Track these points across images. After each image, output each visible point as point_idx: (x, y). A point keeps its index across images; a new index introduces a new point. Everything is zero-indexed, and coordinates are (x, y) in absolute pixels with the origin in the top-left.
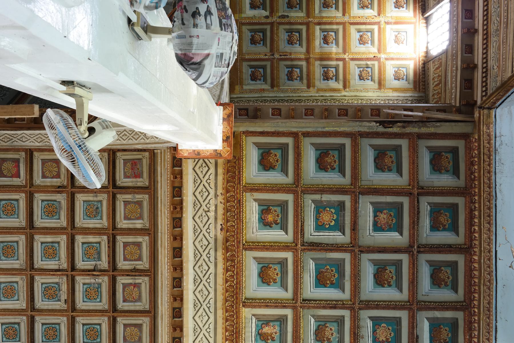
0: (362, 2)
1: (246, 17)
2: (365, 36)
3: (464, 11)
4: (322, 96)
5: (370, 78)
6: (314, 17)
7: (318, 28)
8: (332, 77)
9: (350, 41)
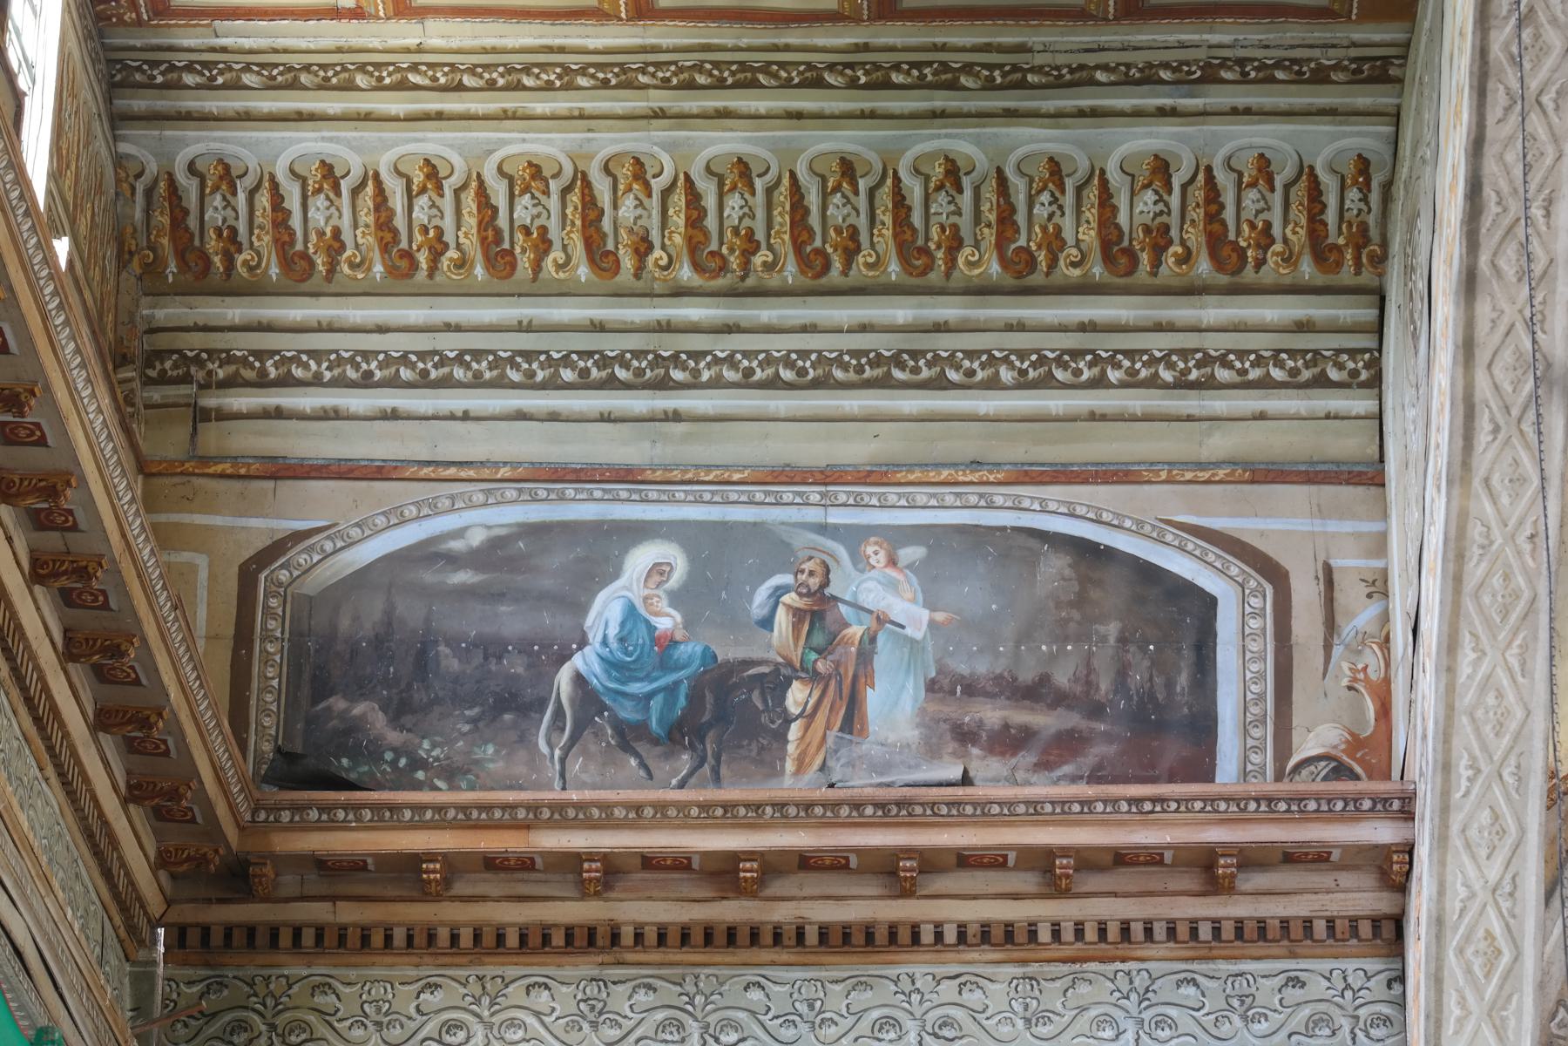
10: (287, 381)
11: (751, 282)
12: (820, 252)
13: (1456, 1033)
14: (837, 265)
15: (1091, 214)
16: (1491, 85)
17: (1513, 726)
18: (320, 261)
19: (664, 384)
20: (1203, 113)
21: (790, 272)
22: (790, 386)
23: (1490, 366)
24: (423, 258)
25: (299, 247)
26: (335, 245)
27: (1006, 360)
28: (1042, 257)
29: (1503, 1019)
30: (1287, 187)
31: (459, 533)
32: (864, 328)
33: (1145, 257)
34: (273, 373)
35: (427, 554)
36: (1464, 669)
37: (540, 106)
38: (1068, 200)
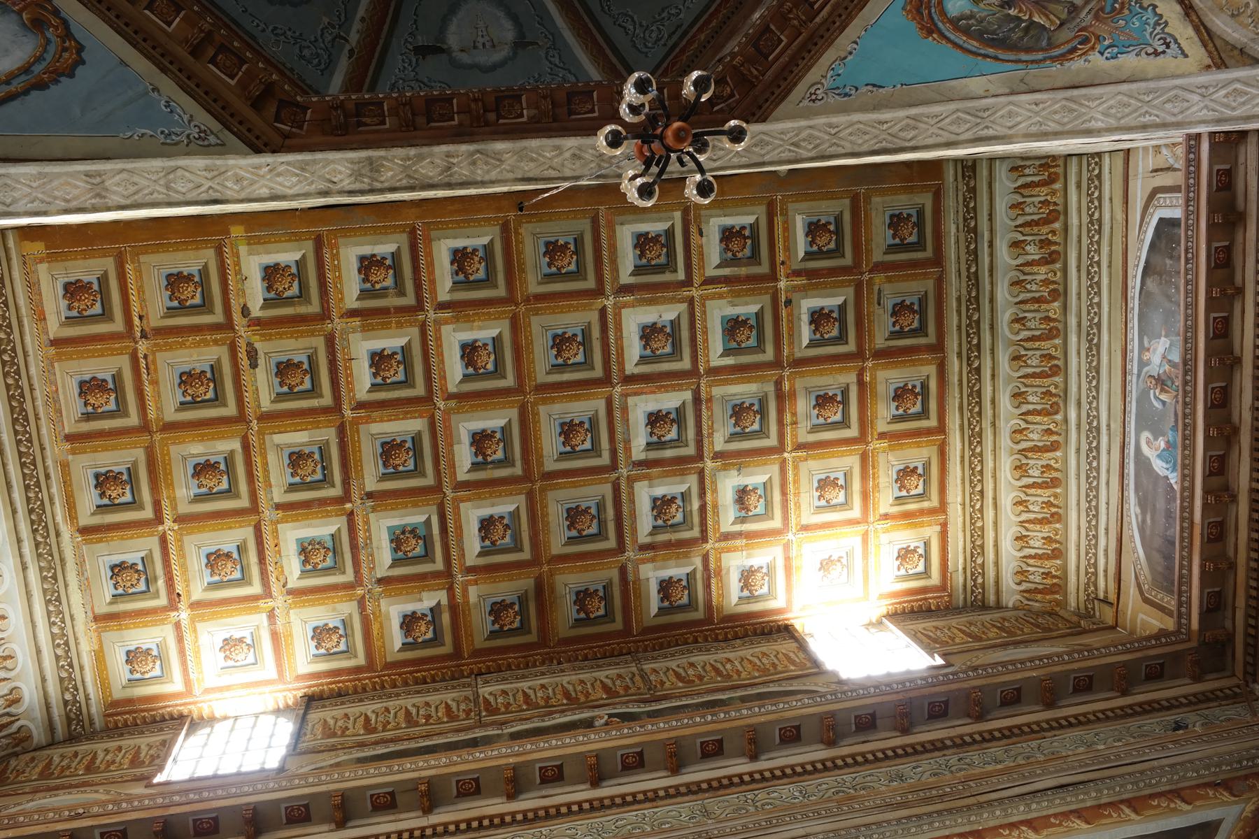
0: (317, 546)
1: (238, 257)
2: (230, 565)
3: (122, 828)
4: (47, 477)
5: (120, 591)
6: (261, 433)
7: (236, 445)
8: (107, 494)
9: (210, 531)
10: (1095, 565)
11: (1061, 394)
12: (1050, 368)
14: (1056, 362)
15: (1035, 269)
16: (827, 153)
17: (1125, 99)
18: (1055, 546)
19: (1098, 429)
20: (991, 231)
21: (1058, 379)
22: (1098, 382)
24: (1054, 510)
26: (1048, 540)
27: (1091, 300)
28: (1052, 287)
30: (1024, 197)
31: (1136, 516)
32: (1079, 353)
33: (1053, 248)
34: (1092, 570)
36: (1100, 124)
37: (989, 464)
38: (1029, 278)
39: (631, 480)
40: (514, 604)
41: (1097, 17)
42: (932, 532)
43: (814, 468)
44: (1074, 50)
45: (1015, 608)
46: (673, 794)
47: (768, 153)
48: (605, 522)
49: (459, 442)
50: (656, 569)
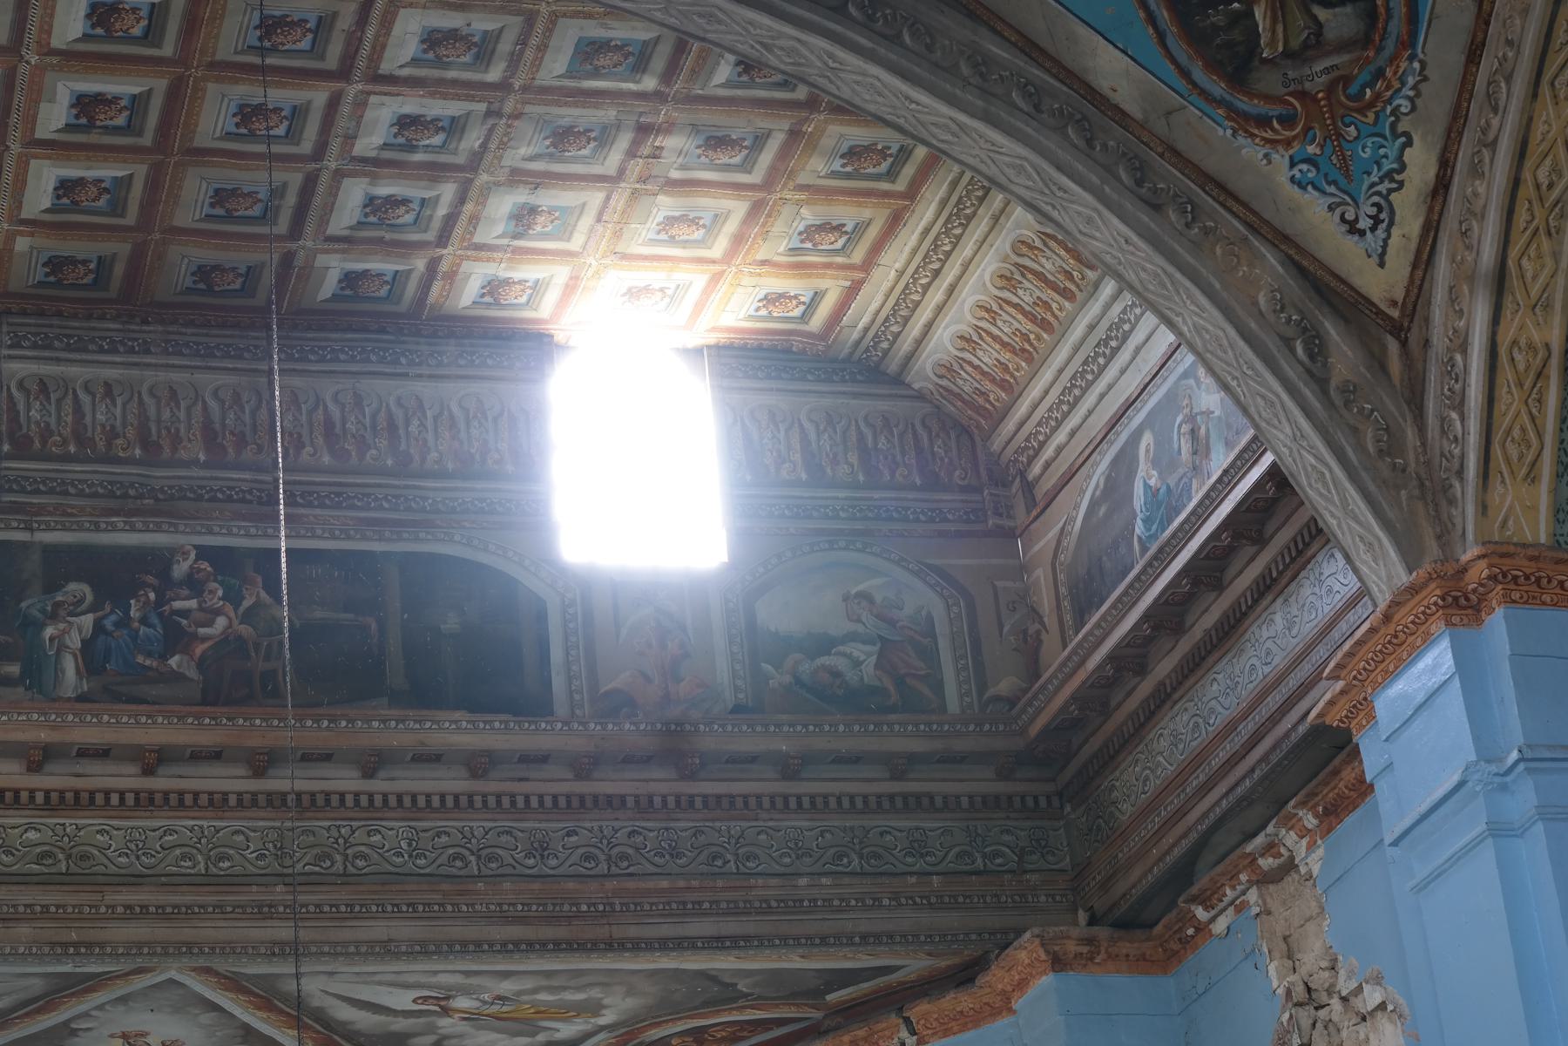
10: (1042, 444)
13: (1343, 534)
16: (811, 80)
17: (1225, 342)
23: (1011, 181)
24: (1027, 347)
25: (998, 378)
29: (1352, 510)
35: (1093, 505)
36: (1185, 329)
37: (967, 249)
39: (339, 175)
40: (91, 261)
41: (1330, 89)
42: (833, 288)
43: (666, 205)
44: (1264, 122)
45: (920, 396)
46: (248, 802)
47: (715, 32)
48: (278, 208)
49: (52, 100)
50: (345, 260)
